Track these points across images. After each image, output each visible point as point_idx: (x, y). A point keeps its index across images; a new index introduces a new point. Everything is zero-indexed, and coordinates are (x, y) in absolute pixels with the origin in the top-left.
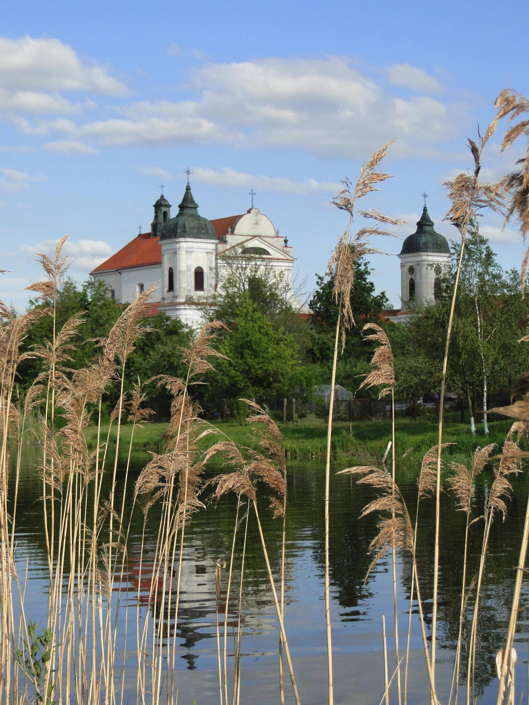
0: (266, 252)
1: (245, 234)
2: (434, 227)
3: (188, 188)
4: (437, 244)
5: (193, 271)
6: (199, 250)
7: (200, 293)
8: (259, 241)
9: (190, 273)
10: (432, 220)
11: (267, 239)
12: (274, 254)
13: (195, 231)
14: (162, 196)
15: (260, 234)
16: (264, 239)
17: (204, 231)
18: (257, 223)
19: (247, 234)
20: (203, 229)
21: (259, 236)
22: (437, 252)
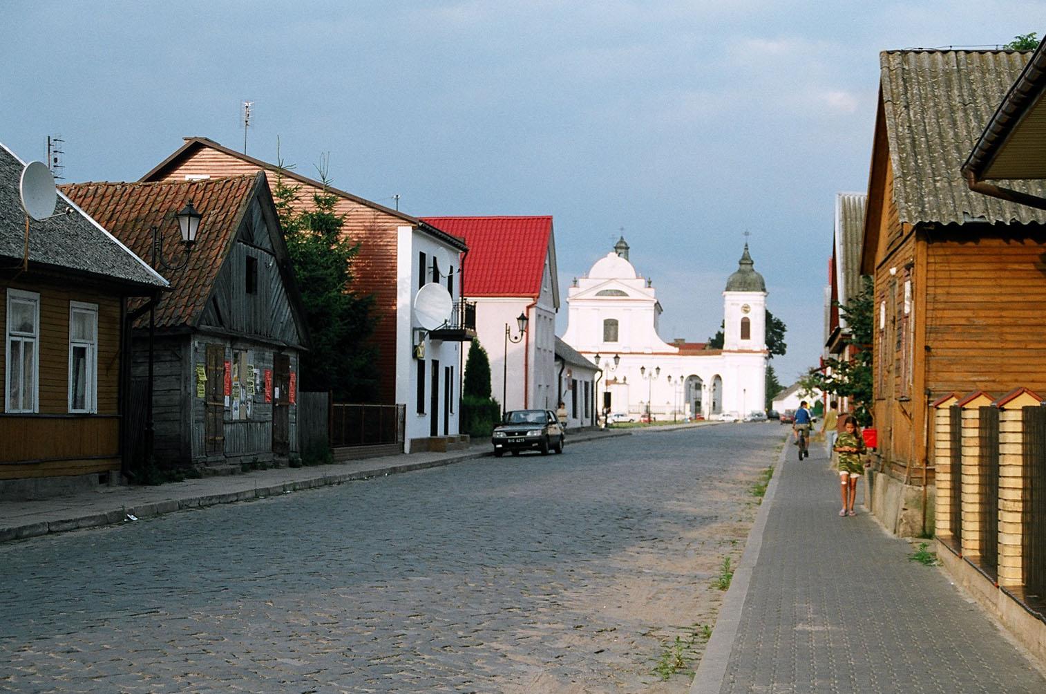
4: (745, 282)
10: (752, 258)
11: (625, 282)
12: (632, 295)
14: (622, 238)
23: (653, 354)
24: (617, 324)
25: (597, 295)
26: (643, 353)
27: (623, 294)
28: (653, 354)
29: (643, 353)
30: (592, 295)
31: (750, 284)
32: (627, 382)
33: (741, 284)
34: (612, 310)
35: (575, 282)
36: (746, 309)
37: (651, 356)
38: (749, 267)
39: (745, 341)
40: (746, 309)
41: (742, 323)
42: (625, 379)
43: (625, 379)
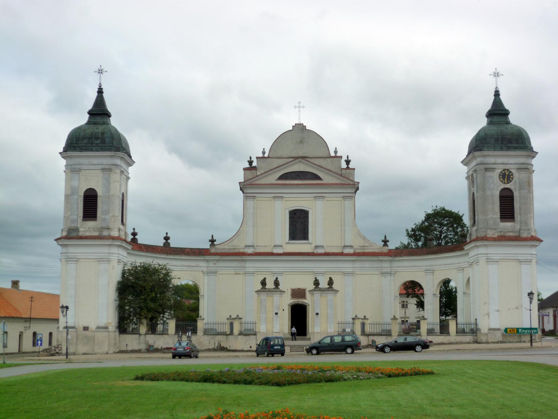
0: (317, 177)
1: (284, 156)
2: (510, 116)
3: (100, 91)
5: (82, 194)
6: (91, 167)
7: (91, 224)
8: (304, 163)
9: (76, 197)
11: (317, 161)
12: (326, 178)
15: (306, 155)
16: (312, 160)
17: (98, 142)
18: (301, 142)
19: (287, 156)
20: (97, 138)
21: (303, 158)
23: (355, 254)
24: (308, 217)
25: (281, 178)
26: (342, 254)
29: (342, 254)
30: (273, 179)
31: (510, 141)
32: (335, 286)
33: (497, 140)
34: (299, 199)
35: (251, 162)
37: (354, 258)
38: (502, 119)
39: (508, 224)
40: (506, 176)
41: (501, 197)
42: (331, 282)
43: (331, 282)
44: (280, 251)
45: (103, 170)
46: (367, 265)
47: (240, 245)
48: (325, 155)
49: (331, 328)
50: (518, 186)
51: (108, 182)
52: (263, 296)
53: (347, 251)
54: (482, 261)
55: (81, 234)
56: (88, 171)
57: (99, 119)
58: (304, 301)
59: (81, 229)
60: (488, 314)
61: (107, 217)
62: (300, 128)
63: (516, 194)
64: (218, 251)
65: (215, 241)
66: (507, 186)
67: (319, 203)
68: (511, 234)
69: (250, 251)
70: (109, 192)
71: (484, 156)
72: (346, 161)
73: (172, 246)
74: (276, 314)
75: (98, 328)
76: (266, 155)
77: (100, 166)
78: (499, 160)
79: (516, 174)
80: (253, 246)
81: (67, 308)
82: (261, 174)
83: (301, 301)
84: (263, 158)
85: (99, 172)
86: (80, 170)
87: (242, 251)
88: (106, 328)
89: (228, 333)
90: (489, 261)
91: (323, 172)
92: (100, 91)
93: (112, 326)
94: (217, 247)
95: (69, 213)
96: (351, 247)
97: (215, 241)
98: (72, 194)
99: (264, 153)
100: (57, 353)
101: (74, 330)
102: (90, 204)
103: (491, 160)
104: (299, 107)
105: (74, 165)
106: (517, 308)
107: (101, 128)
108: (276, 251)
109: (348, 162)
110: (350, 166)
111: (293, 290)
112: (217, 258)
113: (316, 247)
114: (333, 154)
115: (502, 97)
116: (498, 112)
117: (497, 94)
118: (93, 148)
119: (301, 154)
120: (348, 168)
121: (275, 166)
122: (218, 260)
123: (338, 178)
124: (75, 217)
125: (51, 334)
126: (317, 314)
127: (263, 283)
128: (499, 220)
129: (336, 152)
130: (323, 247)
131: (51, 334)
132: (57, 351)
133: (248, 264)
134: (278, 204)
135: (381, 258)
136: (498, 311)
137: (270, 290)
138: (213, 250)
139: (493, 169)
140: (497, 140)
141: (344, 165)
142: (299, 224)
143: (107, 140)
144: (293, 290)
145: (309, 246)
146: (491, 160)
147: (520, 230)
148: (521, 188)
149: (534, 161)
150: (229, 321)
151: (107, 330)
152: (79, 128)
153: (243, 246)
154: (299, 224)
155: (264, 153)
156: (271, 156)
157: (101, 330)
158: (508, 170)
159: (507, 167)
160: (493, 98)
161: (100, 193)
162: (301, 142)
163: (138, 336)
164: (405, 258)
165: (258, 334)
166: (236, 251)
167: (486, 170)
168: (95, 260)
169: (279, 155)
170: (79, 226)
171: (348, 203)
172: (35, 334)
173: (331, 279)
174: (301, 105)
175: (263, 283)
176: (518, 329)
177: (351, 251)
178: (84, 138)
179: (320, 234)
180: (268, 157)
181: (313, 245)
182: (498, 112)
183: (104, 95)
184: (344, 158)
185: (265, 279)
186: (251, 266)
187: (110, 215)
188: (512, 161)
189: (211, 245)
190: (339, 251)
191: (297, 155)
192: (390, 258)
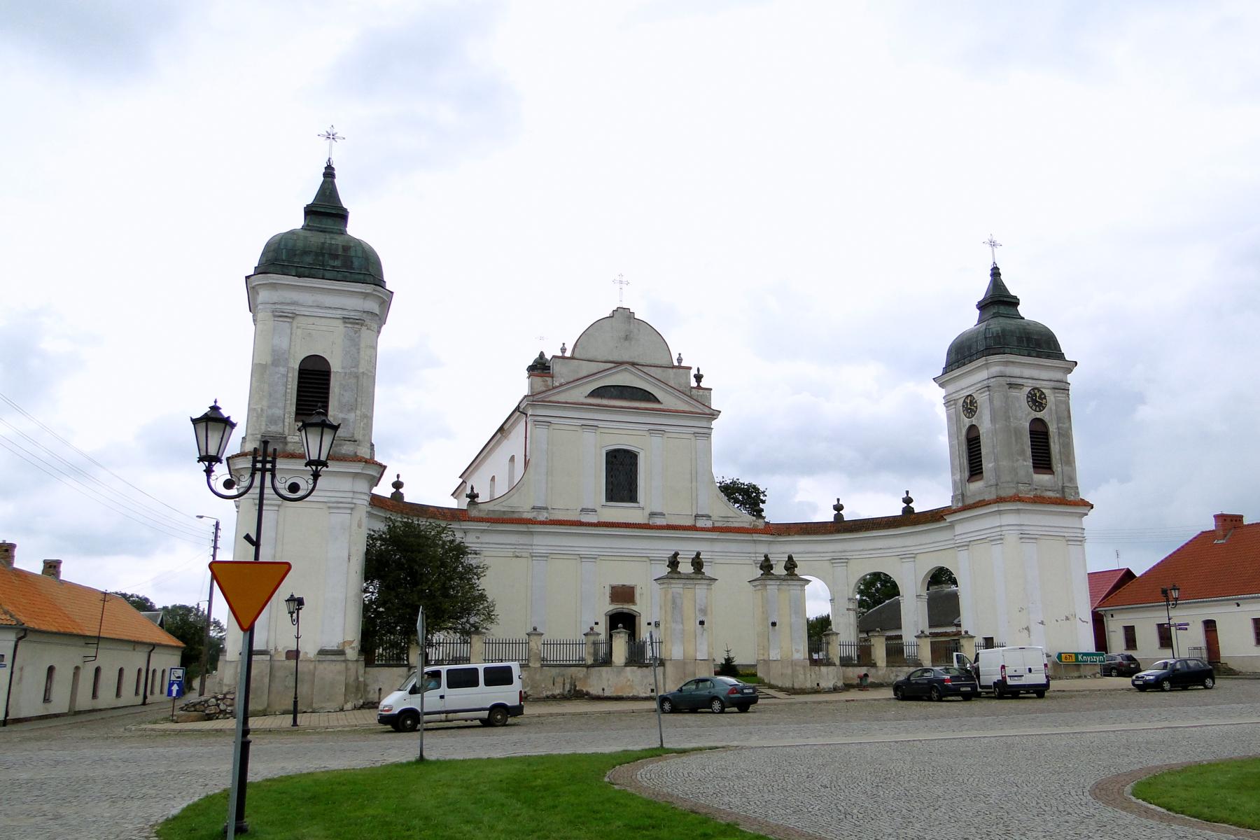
2: (1021, 309)
3: (329, 173)
6: (321, 312)
8: (632, 373)
9: (282, 370)
11: (652, 371)
12: (668, 400)
13: (309, 259)
15: (635, 361)
16: (645, 369)
17: (337, 263)
18: (627, 338)
22: (1029, 355)
23: (714, 529)
25: (594, 394)
26: (693, 528)
27: (648, 397)
28: (714, 529)
29: (693, 528)
30: (580, 394)
31: (1038, 344)
33: (1020, 340)
34: (624, 430)
36: (1036, 400)
39: (1044, 478)
40: (1036, 400)
41: (1032, 432)
44: (592, 518)
45: (345, 320)
46: (733, 547)
47: (524, 505)
48: (664, 362)
49: (798, 651)
50: (1054, 416)
51: (354, 343)
52: (677, 587)
53: (700, 524)
54: (1011, 537)
55: (290, 448)
56: (311, 320)
57: (328, 223)
58: (633, 607)
59: (289, 439)
60: (1027, 629)
61: (351, 416)
62: (623, 316)
63: (1052, 429)
64: (482, 515)
65: (477, 496)
66: (1039, 415)
67: (656, 440)
68: (1050, 494)
69: (543, 516)
70: (357, 366)
71: (1007, 363)
72: (695, 376)
73: (406, 499)
74: (702, 623)
75: (322, 652)
76: (568, 354)
77: (339, 312)
78: (1027, 372)
79: (1051, 397)
80: (546, 509)
81: (300, 602)
82: (561, 385)
83: (627, 607)
84: (563, 358)
85: (339, 323)
86: (294, 316)
87: (526, 516)
88: (341, 652)
89: (590, 662)
90: (1024, 537)
91: (664, 390)
92: (329, 173)
93: (353, 648)
94: (482, 506)
95: (265, 403)
96: (709, 517)
97: (477, 496)
98: (275, 363)
99: (563, 350)
100: (221, 711)
101: (268, 658)
102: (313, 384)
103: (1016, 371)
104: (621, 282)
105: (282, 303)
106: (1067, 619)
107: (339, 240)
108: (586, 518)
109: (699, 378)
110: (702, 385)
111: (613, 588)
112: (484, 526)
113: (652, 514)
114: (676, 363)
115: (1004, 278)
116: (999, 301)
117: (995, 273)
118: (327, 274)
119: (626, 359)
120: (699, 387)
121: (584, 373)
122: (483, 531)
123: (688, 403)
124: (278, 412)
125: (121, 670)
126: (774, 624)
127: (674, 563)
128: (1032, 470)
129: (680, 360)
130: (662, 514)
131: (121, 670)
132: (222, 707)
133: (537, 540)
134: (589, 437)
135: (756, 537)
136: (1042, 623)
137: (688, 577)
138: (474, 513)
139: (1018, 386)
140: (1020, 340)
141: (694, 383)
142: (622, 473)
143: (356, 263)
144: (613, 588)
145: (639, 512)
146: (1016, 371)
147: (1063, 487)
148: (1059, 420)
149: (1070, 378)
150: (592, 638)
151: (342, 658)
152: (292, 232)
153: (528, 507)
154: (622, 473)
155: (563, 350)
156: (576, 355)
157: (330, 657)
158: (1038, 390)
159: (1038, 384)
160: (990, 278)
161: (336, 366)
162: (627, 338)
163: (405, 669)
164: (797, 538)
165: (668, 664)
166: (516, 516)
167: (1011, 385)
168: (321, 506)
169: (589, 356)
170: (287, 432)
171: (700, 443)
172: (98, 670)
173: (790, 558)
174: (624, 279)
175: (674, 563)
176: (1077, 654)
177: (709, 524)
178: (305, 252)
179: (656, 491)
180: (572, 358)
181: (647, 512)
182: (999, 301)
183: (338, 182)
184: (694, 372)
185: (676, 554)
186: (543, 542)
187: (358, 412)
188: (1045, 374)
189: (469, 504)
190: (689, 522)
191: (620, 359)
192: (769, 538)
